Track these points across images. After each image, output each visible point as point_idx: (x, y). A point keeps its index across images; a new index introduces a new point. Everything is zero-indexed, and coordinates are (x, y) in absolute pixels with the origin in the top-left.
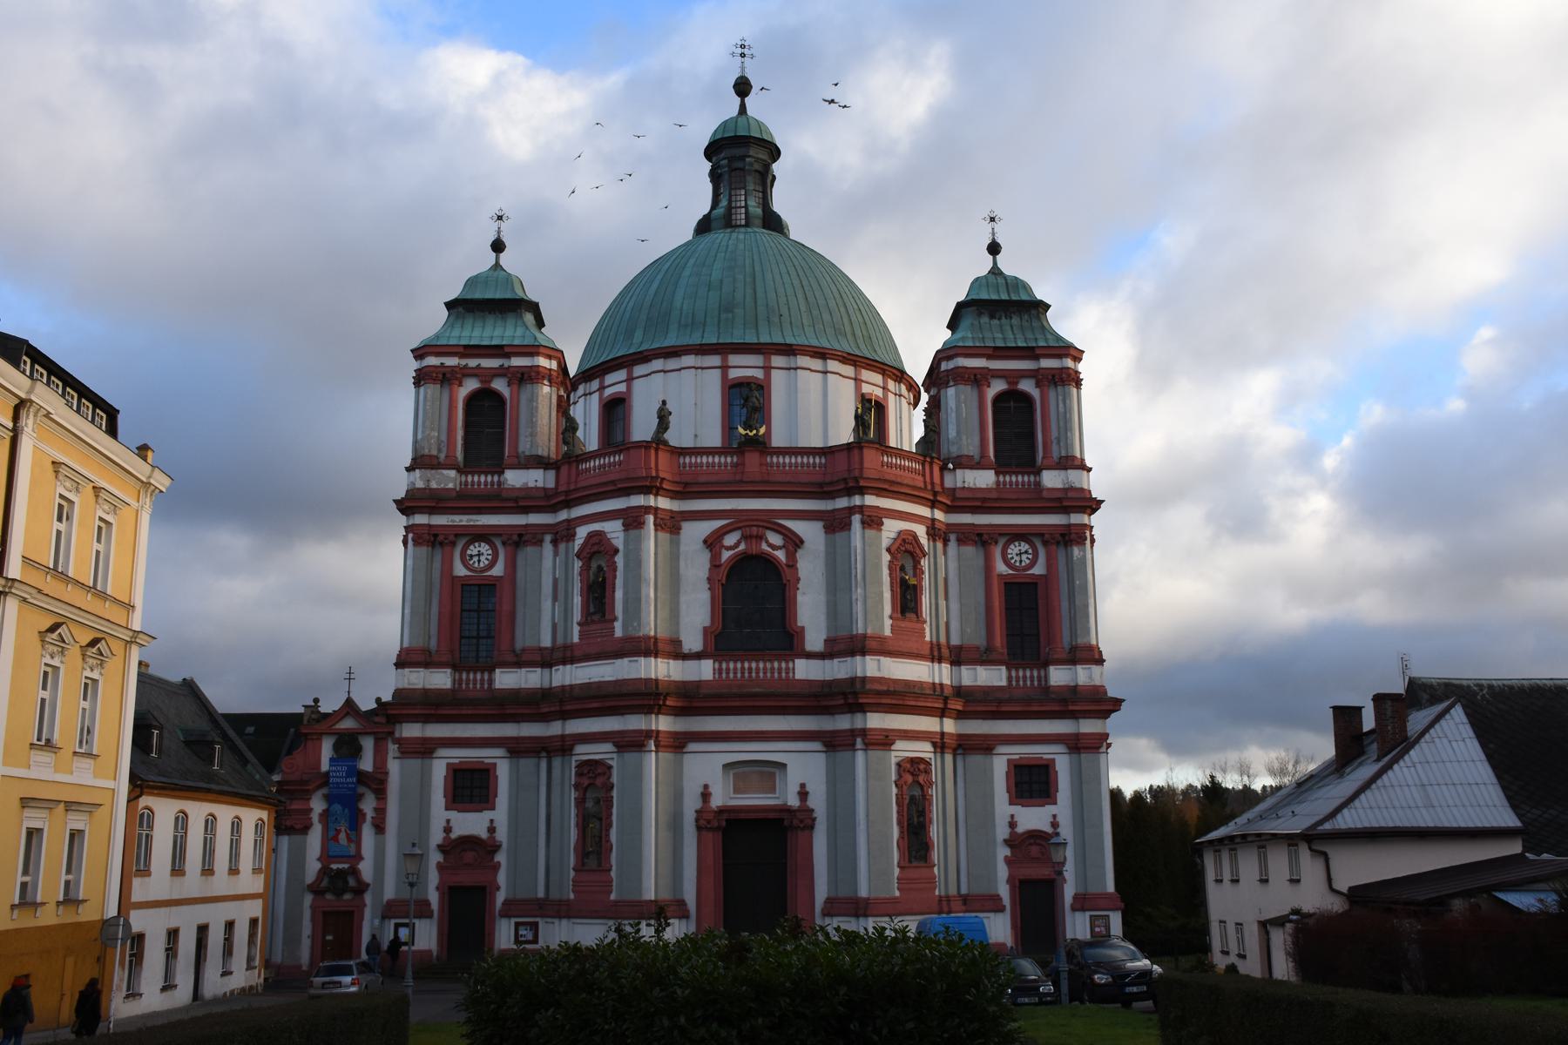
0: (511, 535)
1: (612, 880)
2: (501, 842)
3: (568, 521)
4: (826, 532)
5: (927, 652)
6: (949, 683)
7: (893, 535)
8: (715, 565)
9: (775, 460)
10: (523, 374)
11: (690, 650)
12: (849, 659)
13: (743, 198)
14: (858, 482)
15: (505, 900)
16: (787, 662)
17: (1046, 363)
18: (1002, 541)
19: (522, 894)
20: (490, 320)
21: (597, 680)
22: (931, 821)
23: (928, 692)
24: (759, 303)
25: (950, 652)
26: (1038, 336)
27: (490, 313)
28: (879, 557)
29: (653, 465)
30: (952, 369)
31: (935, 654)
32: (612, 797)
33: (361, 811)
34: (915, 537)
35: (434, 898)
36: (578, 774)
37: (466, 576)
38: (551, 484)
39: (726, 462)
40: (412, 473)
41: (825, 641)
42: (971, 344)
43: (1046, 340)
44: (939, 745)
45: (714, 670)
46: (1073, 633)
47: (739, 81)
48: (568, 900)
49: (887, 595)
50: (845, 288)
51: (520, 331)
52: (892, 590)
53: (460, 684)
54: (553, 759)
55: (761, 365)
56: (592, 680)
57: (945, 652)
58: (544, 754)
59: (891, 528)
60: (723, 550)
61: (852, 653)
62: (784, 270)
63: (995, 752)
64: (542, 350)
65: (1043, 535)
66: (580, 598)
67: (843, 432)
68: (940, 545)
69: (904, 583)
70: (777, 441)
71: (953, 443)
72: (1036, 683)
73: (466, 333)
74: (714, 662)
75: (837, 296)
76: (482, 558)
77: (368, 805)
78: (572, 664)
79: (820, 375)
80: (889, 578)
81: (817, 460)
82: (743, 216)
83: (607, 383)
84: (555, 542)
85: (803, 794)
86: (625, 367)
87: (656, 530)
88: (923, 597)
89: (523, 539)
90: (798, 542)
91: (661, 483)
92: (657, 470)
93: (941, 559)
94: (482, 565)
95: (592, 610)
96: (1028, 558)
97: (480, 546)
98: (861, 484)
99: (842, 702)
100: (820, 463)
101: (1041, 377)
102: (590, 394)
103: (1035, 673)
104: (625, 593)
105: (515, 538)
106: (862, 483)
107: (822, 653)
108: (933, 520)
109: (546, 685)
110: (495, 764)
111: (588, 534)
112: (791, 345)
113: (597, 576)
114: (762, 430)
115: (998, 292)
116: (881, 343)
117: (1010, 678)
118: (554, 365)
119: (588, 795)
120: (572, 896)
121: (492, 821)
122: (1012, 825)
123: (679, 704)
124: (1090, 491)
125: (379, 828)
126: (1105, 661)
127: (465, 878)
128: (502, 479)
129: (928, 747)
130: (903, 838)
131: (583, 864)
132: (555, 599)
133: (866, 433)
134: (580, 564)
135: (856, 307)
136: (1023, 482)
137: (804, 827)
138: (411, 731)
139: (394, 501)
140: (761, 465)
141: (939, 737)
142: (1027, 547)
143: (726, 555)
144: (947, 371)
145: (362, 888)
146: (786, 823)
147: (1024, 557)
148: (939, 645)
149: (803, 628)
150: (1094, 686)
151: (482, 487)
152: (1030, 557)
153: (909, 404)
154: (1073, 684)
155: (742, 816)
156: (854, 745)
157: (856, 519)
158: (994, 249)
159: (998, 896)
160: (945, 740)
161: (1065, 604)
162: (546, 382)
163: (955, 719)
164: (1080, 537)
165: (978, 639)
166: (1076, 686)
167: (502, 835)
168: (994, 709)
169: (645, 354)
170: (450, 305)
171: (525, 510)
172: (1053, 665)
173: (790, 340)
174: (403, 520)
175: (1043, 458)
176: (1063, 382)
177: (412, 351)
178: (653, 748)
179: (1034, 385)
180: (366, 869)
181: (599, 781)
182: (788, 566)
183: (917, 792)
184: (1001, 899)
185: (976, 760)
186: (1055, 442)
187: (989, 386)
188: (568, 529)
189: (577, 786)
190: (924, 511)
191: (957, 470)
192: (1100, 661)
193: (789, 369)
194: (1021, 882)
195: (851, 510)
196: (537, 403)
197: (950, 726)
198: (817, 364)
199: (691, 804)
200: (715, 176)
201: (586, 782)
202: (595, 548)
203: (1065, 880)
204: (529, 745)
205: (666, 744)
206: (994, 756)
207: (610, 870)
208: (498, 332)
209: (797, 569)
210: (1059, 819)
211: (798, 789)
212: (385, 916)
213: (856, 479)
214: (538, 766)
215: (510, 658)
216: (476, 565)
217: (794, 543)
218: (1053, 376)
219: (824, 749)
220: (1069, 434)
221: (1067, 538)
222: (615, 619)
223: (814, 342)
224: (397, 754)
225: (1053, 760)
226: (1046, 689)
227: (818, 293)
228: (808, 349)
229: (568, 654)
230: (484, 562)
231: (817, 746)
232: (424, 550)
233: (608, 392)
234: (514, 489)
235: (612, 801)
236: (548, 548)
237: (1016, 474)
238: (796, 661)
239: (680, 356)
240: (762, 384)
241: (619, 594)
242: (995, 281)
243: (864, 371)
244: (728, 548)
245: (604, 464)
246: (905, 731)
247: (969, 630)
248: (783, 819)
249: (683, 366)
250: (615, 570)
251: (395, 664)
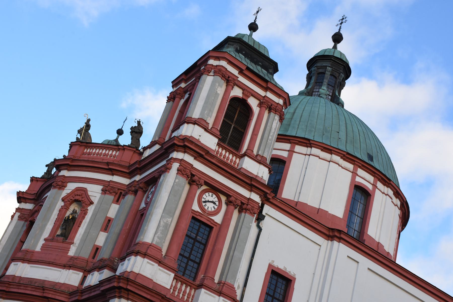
65: (230, 196)
96: (214, 207)
103: (188, 291)
142: (216, 199)
147: (211, 205)
152: (216, 207)
176: (276, 111)
221: (244, 206)
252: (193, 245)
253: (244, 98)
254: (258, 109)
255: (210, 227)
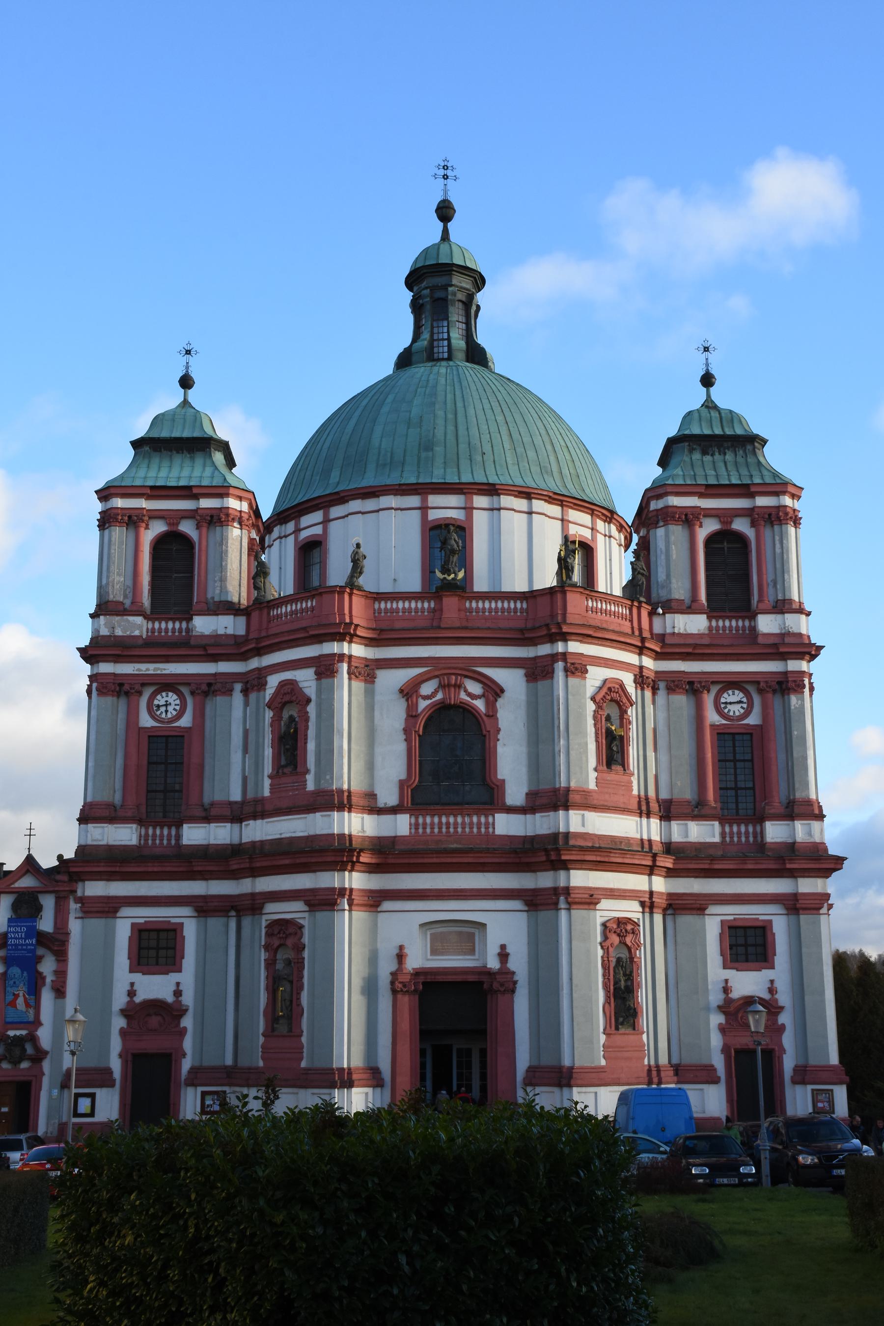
0: (201, 684)
1: (303, 1048)
2: (188, 1006)
3: (259, 670)
4: (528, 681)
5: (634, 806)
6: (658, 839)
7: (598, 684)
8: (412, 715)
9: (474, 605)
10: (212, 517)
11: (386, 804)
12: (552, 814)
13: (445, 330)
14: (561, 628)
15: (191, 1068)
16: (486, 817)
17: (762, 501)
18: (714, 689)
19: (210, 1061)
20: (177, 459)
21: (288, 835)
22: (639, 985)
23: (635, 848)
24: (461, 440)
25: (660, 806)
26: (754, 473)
27: (178, 452)
28: (583, 707)
29: (347, 611)
30: (662, 509)
31: (643, 809)
32: (304, 958)
33: (41, 974)
34: (622, 686)
35: (116, 1065)
36: (268, 935)
37: (153, 727)
38: (241, 631)
39: (423, 608)
40: (96, 620)
41: (527, 794)
42: (682, 482)
43: (762, 477)
44: (648, 904)
45: (410, 825)
46: (791, 787)
47: (441, 205)
48: (257, 1068)
49: (592, 747)
50: (552, 424)
51: (209, 471)
52: (597, 741)
53: (146, 840)
54: (242, 918)
55: (463, 505)
56: (283, 836)
57: (654, 806)
58: (233, 913)
59: (596, 676)
60: (420, 701)
61: (555, 808)
62: (487, 406)
63: (707, 912)
64: (232, 491)
65: (758, 683)
66: (271, 750)
67: (547, 578)
68: (648, 694)
69: (610, 735)
70: (481, 584)
71: (663, 587)
72: (751, 839)
73: (152, 473)
74: (410, 818)
75: (543, 432)
76: (170, 709)
77: (47, 967)
78: (263, 819)
79: (525, 516)
80: (593, 730)
81: (519, 605)
82: (446, 349)
83: (303, 525)
84: (245, 692)
85: (503, 955)
86: (319, 509)
87: (350, 679)
88: (631, 748)
89: (212, 688)
90: (498, 691)
91: (355, 630)
92: (351, 617)
93: (650, 709)
94: (169, 716)
95: (283, 762)
96: (742, 707)
97: (167, 696)
98: (564, 630)
99: (544, 858)
100: (522, 608)
101: (755, 516)
102: (286, 536)
103: (751, 829)
104: (318, 745)
105: (204, 687)
106: (565, 629)
107: (523, 807)
108: (641, 668)
109: (236, 841)
110: (182, 924)
111: (280, 683)
112: (494, 485)
113: (288, 726)
114: (461, 575)
115: (712, 428)
116: (590, 482)
117: (723, 834)
118: (245, 506)
119: (279, 956)
120: (261, 1064)
121: (178, 984)
122: (726, 990)
123: (373, 861)
124: (809, 637)
125: (60, 992)
126: (825, 816)
127: (152, 1044)
128: (190, 627)
129: (635, 906)
130: (609, 1003)
131: (273, 1030)
132: (245, 750)
133: (569, 577)
134: (271, 714)
135: (563, 444)
136: (737, 627)
137: (505, 990)
138: (94, 889)
139: (79, 649)
140: (459, 610)
141: (647, 896)
142: (741, 695)
143: (423, 704)
144: (657, 510)
145: (40, 1056)
146: (485, 986)
148: (647, 798)
149: (504, 781)
150: (815, 843)
151: (170, 634)
152: (745, 706)
153: (620, 545)
154: (790, 841)
155: (440, 978)
156: (556, 903)
157: (560, 666)
158: (707, 380)
159: (713, 1066)
160: (654, 900)
161: (782, 757)
162: (236, 524)
163: (665, 877)
164: (798, 686)
165: (686, 791)
166: (794, 843)
167: (188, 999)
168: (707, 866)
169: (342, 495)
170: (137, 444)
171: (214, 658)
172: (769, 820)
173: (493, 479)
174: (86, 669)
175: (758, 602)
177: (96, 492)
178: (347, 907)
179: (749, 524)
180: (44, 1036)
181: (290, 942)
182: (488, 716)
183: (624, 955)
184: (715, 1070)
185: (686, 920)
186: (771, 584)
187: (701, 526)
188: (259, 678)
189: (267, 947)
190: (632, 658)
191: (667, 615)
192: (820, 817)
193: (492, 509)
194: (737, 1052)
195: (554, 658)
196: (227, 547)
197: (660, 884)
198: (521, 504)
199: (386, 967)
200: (417, 307)
201: (276, 943)
202: (287, 698)
203: (785, 1050)
204: (216, 904)
205: (361, 902)
206: (706, 917)
207: (301, 1036)
208: (186, 472)
209: (497, 719)
210: (778, 985)
211: (498, 950)
212: (65, 1085)
213: (559, 626)
214: (227, 926)
215: (199, 812)
216: (164, 716)
217: (494, 691)
218: (770, 515)
219: (526, 908)
220: (786, 576)
221: (784, 686)
222: (307, 771)
223: (519, 481)
224: (80, 915)
225: (770, 922)
226: (761, 846)
227: (523, 430)
228: (512, 488)
229: (259, 809)
230: (172, 712)
231: (517, 904)
232: (109, 700)
233: (304, 534)
234: (203, 636)
235: (303, 963)
236: (238, 698)
237: (730, 618)
238: (496, 815)
239: (378, 496)
240: (463, 525)
241: (311, 746)
242: (708, 415)
243: (571, 512)
244: (426, 698)
245: (296, 610)
246: (611, 890)
247: (679, 783)
248: (482, 983)
249: (381, 507)
250: (307, 720)
251: (78, 820)
252: (735, 768)
253: (725, 528)
254: (753, 530)
255: (750, 733)
